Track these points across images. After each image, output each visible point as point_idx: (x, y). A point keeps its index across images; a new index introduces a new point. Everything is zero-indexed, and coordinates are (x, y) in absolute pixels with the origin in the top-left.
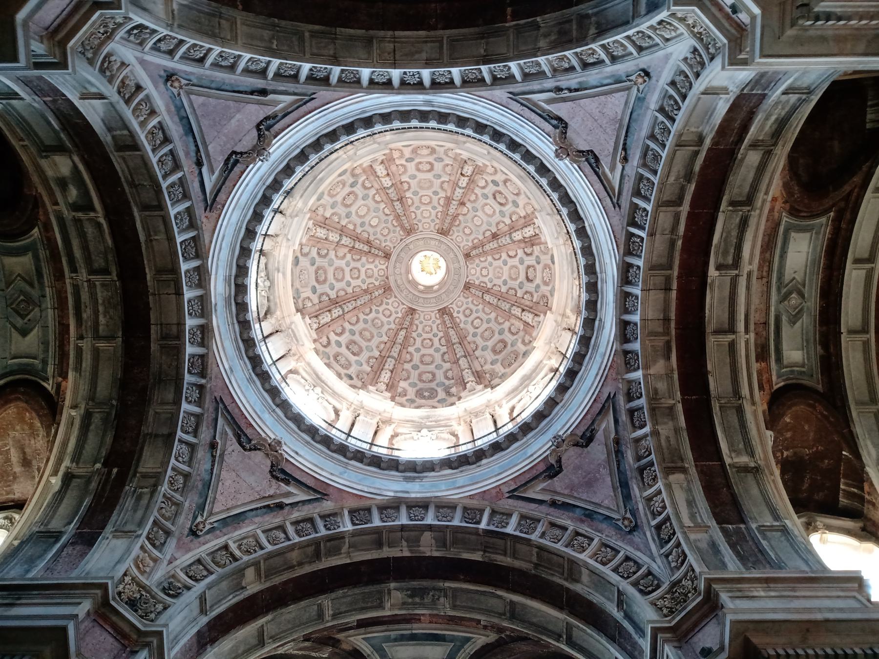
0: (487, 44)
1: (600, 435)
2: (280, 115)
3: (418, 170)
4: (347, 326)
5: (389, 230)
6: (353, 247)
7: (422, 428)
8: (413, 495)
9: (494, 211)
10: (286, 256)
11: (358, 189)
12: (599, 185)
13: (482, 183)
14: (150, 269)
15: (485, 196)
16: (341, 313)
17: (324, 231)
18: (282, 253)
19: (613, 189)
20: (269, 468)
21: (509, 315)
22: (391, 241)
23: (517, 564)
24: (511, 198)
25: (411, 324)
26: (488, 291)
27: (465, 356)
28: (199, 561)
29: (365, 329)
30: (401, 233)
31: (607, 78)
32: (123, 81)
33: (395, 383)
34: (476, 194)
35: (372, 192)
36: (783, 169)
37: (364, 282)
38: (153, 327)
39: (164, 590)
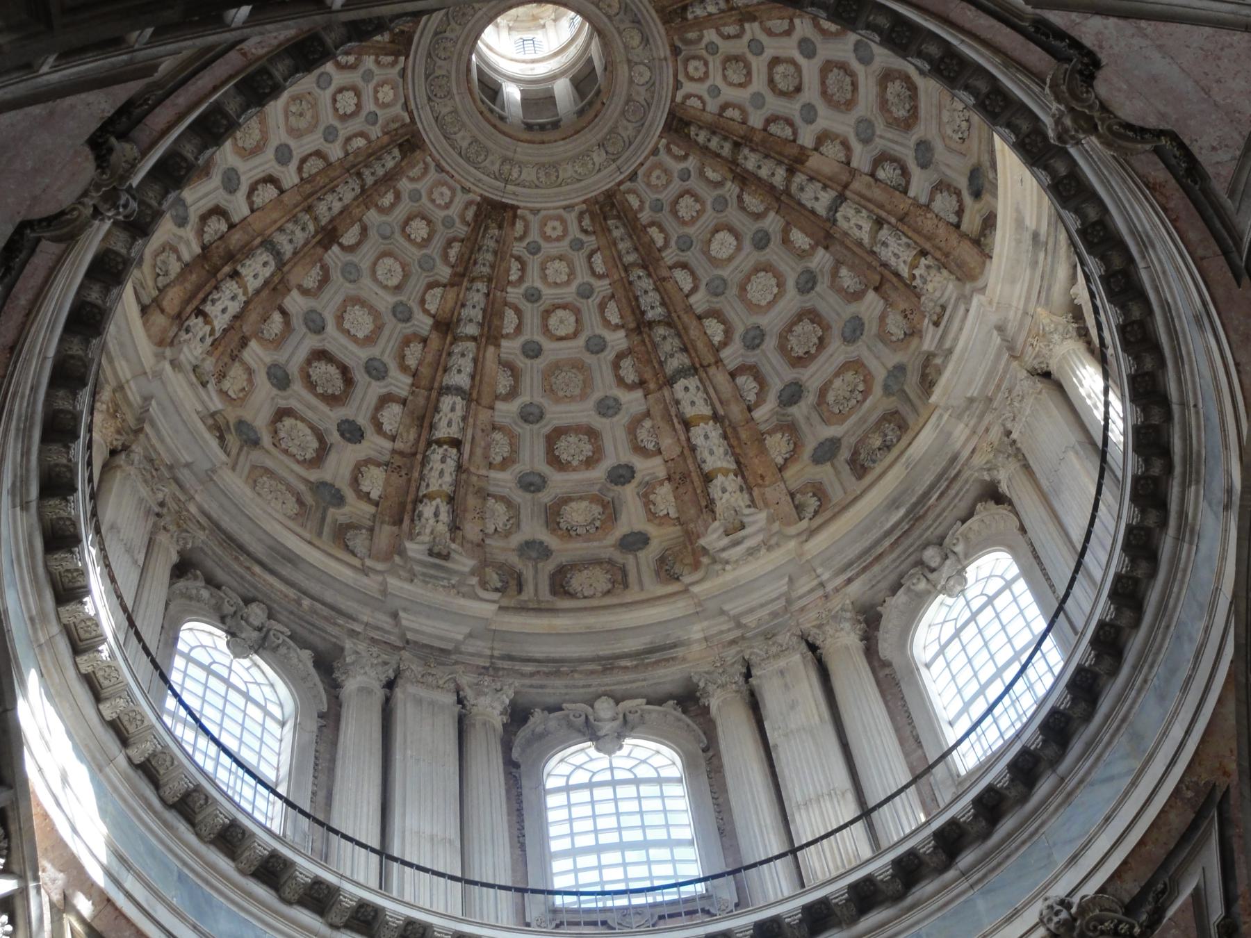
3: (592, 434)
6: (791, 171)
9: (340, 319)
11: (779, 374)
13: (392, 416)
15: (376, 370)
17: (885, 254)
18: (1019, 290)
20: (1101, 75)
22: (666, 171)
24: (298, 397)
30: (634, 202)
34: (404, 368)
35: (733, 355)
37: (756, 47)
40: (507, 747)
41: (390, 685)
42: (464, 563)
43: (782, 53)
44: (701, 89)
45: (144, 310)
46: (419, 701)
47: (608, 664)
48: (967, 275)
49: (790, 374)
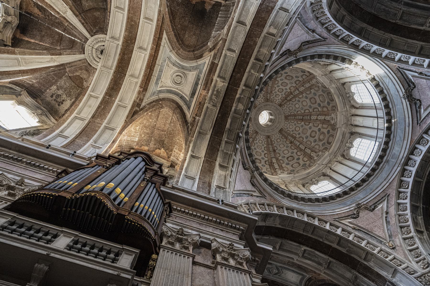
0: (416, 195)
3: (313, 131)
6: (292, 94)
9: (284, 154)
10: (316, 72)
11: (316, 106)
12: (343, 215)
13: (299, 153)
14: (395, 37)
15: (292, 153)
17: (307, 86)
18: (318, 71)
23: (223, 143)
24: (291, 163)
26: (253, 141)
31: (391, 233)
34: (294, 150)
35: (311, 110)
36: (332, 281)
38: (372, 28)
40: (346, 159)
41: (331, 169)
42: (320, 153)
45: (272, 175)
46: (334, 166)
47: (342, 142)
48: (314, 77)
49: (317, 104)
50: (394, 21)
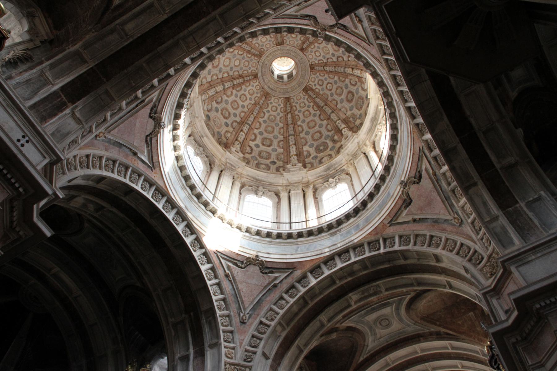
1: (424, 173)
2: (157, 103)
4: (256, 131)
5: (248, 61)
6: (234, 85)
7: (329, 178)
8: (339, 245)
10: (202, 126)
16: (248, 127)
18: (199, 126)
19: (363, 38)
20: (259, 271)
21: (346, 75)
22: (253, 67)
23: (409, 262)
25: (291, 107)
26: (326, 64)
27: (333, 112)
28: (253, 336)
29: (266, 127)
30: (256, 58)
32: (80, 162)
33: (301, 150)
37: (251, 99)
39: (245, 360)
43: (246, 102)
44: (255, 85)
50: (138, 229)
